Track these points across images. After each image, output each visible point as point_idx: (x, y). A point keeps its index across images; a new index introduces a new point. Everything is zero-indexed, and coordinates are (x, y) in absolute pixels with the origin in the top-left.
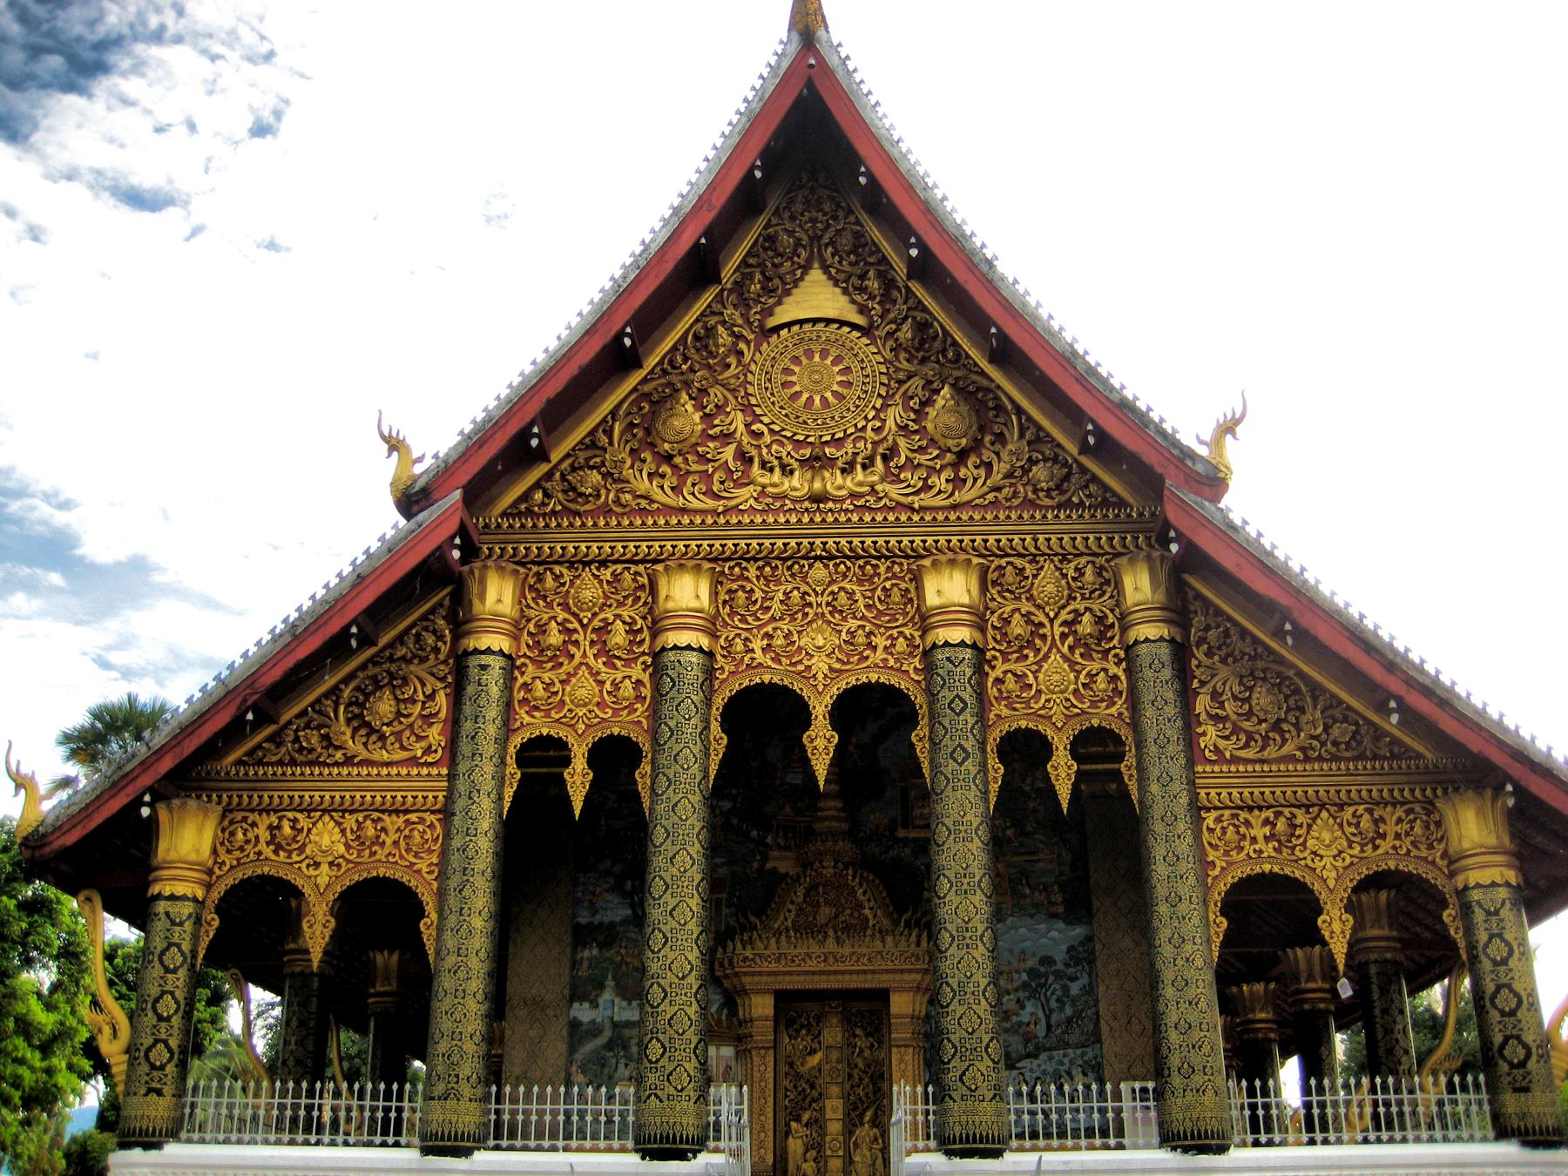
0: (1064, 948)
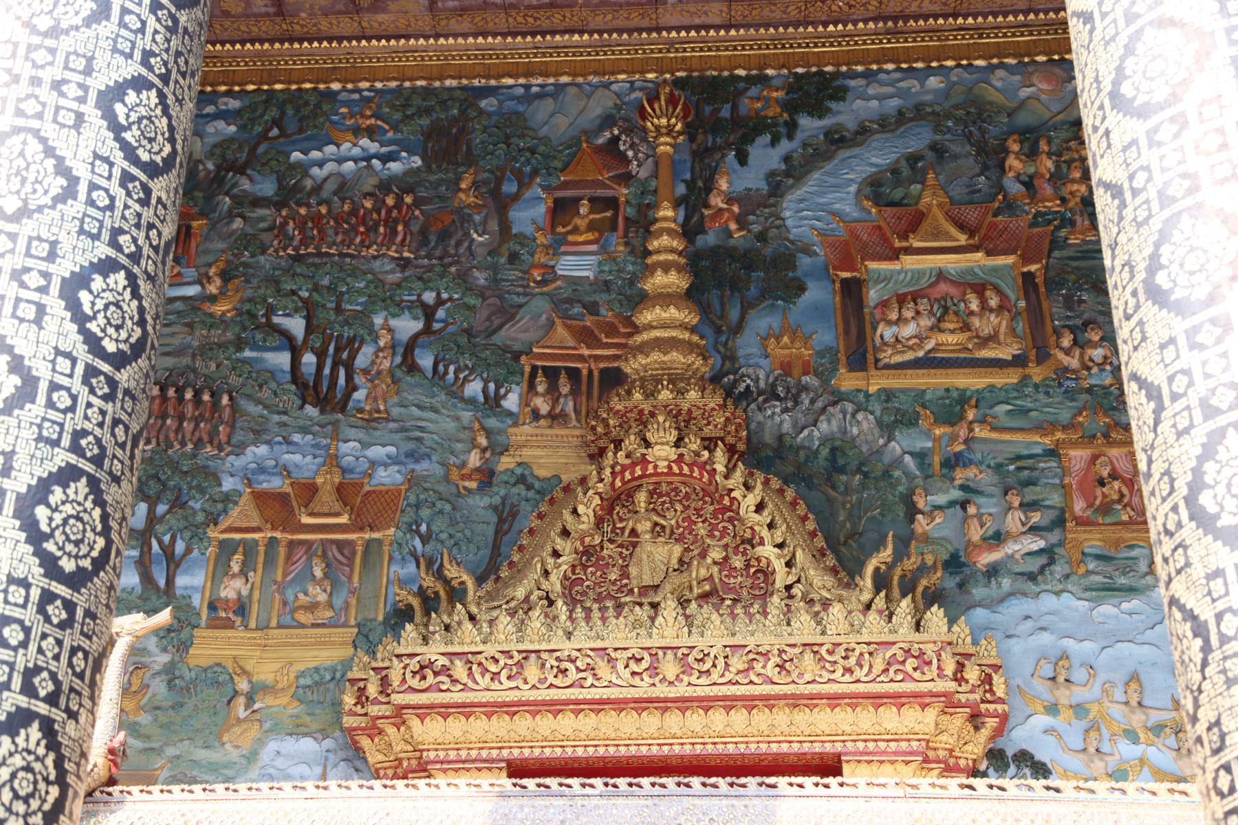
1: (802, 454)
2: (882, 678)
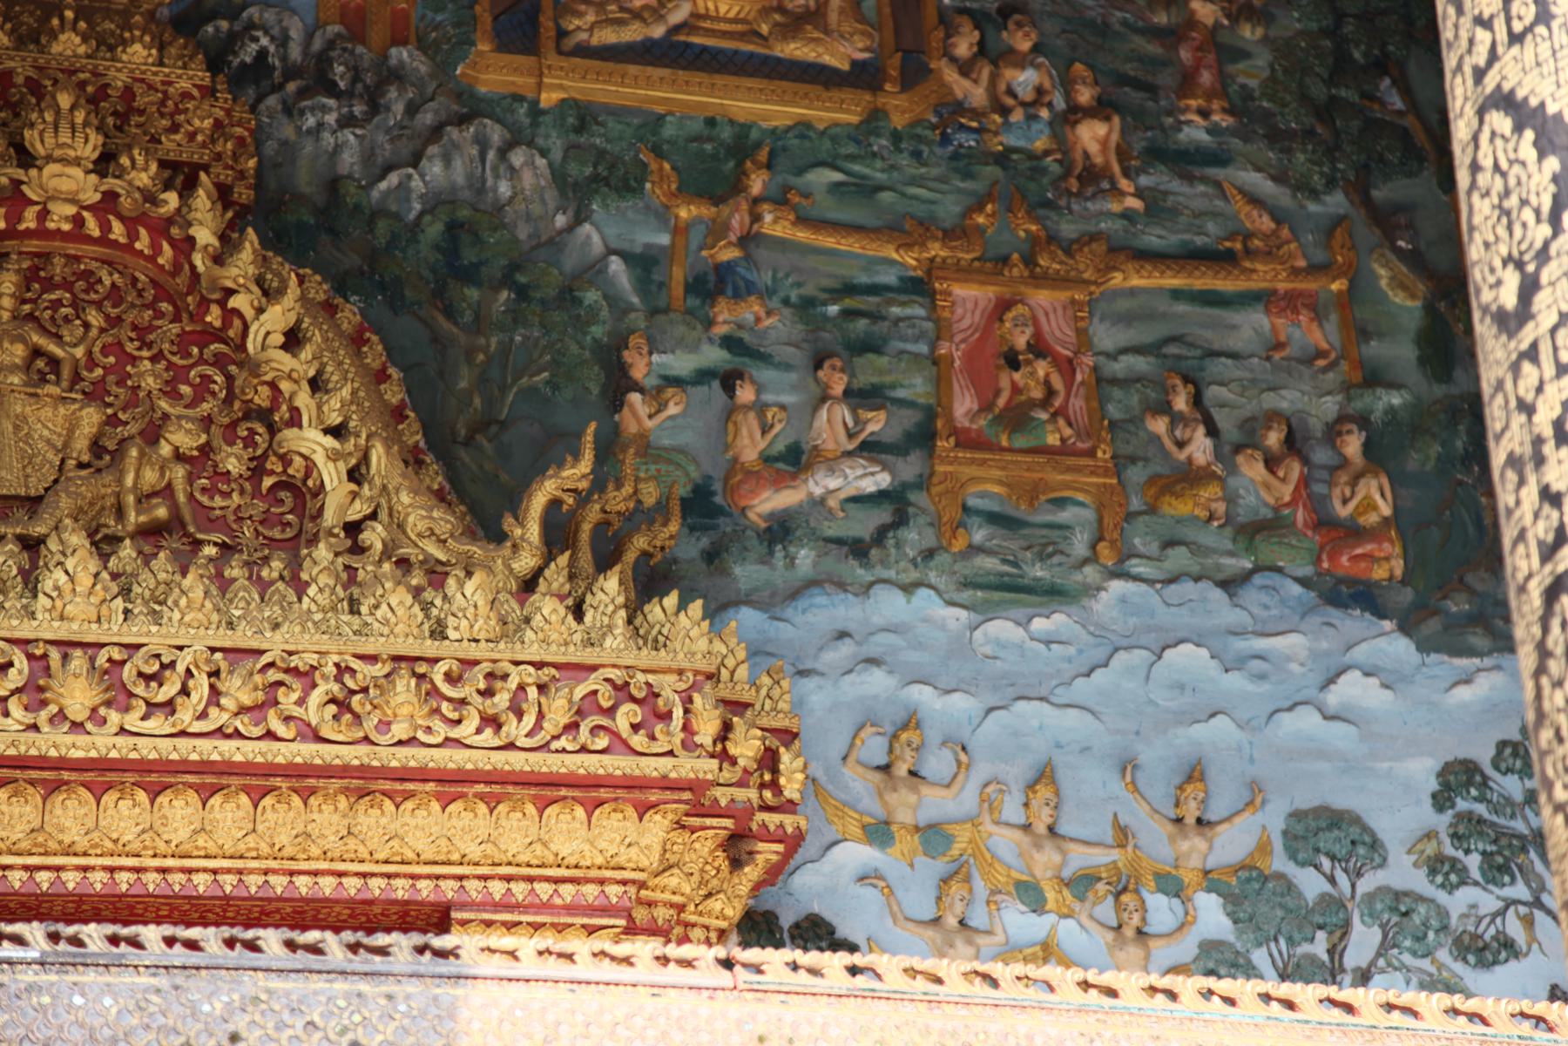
0: (1423, 772)
1: (382, 226)
2: (562, 743)
